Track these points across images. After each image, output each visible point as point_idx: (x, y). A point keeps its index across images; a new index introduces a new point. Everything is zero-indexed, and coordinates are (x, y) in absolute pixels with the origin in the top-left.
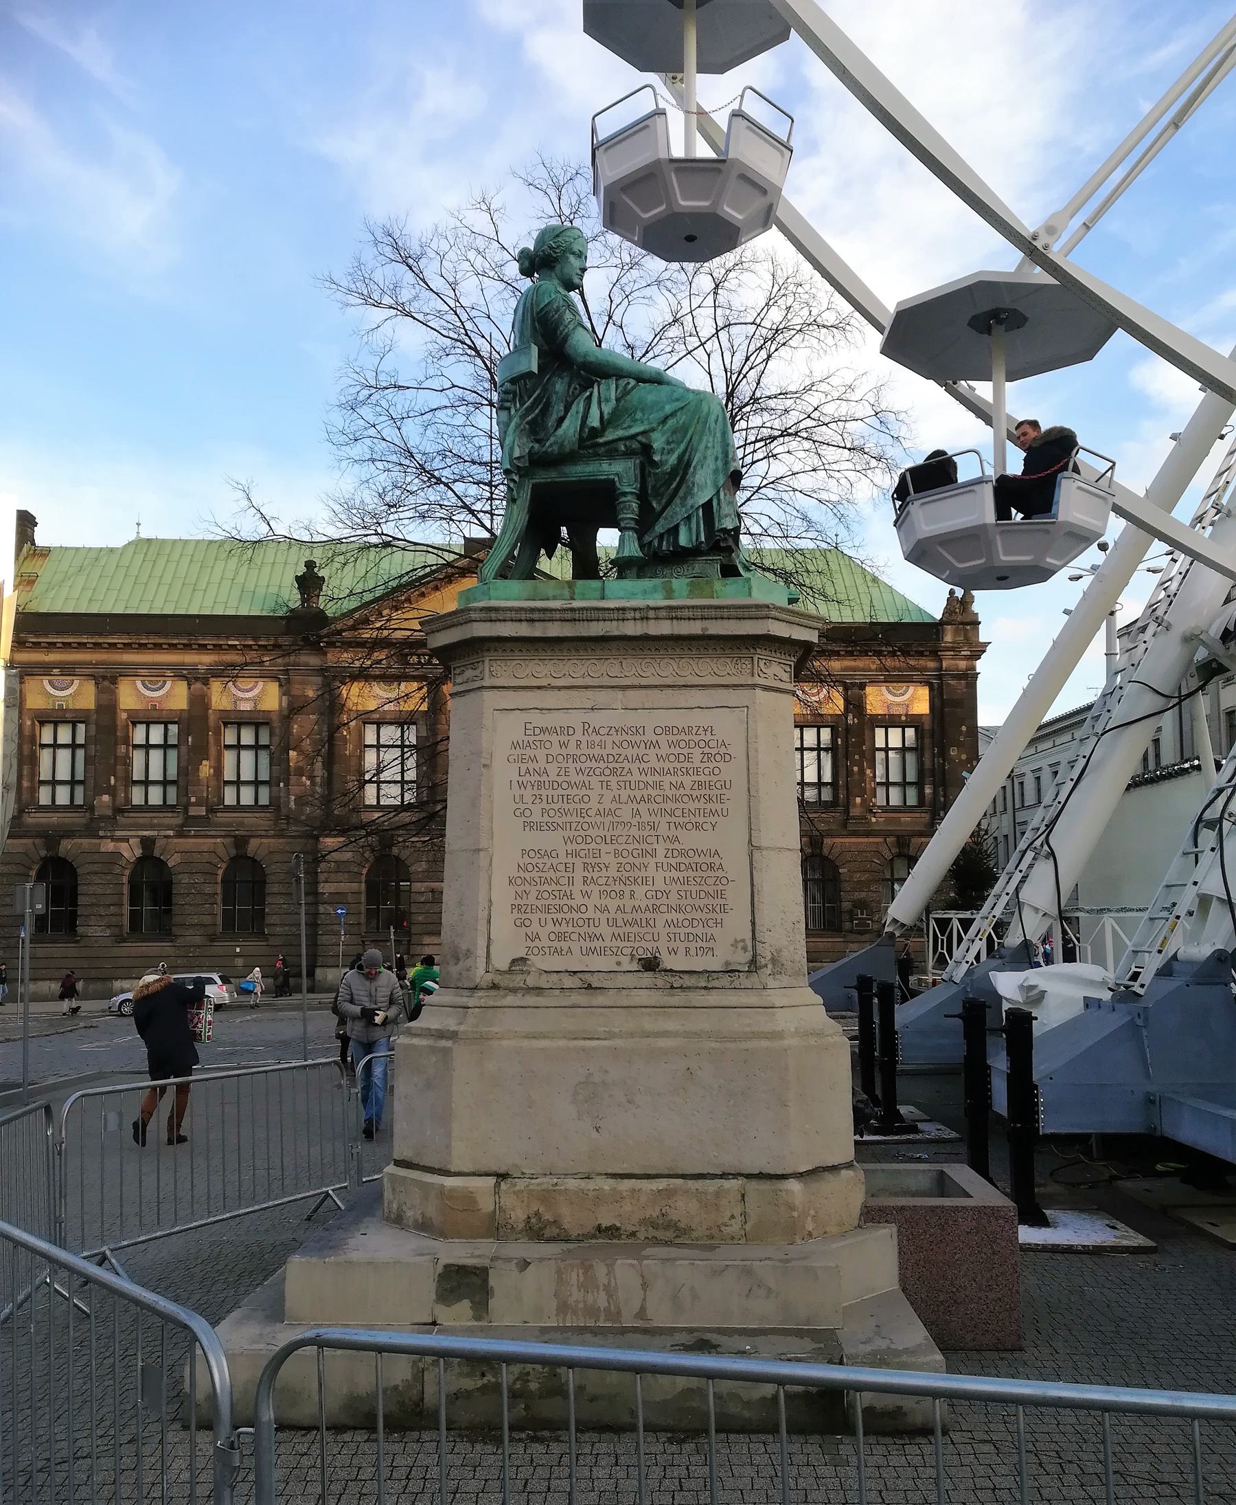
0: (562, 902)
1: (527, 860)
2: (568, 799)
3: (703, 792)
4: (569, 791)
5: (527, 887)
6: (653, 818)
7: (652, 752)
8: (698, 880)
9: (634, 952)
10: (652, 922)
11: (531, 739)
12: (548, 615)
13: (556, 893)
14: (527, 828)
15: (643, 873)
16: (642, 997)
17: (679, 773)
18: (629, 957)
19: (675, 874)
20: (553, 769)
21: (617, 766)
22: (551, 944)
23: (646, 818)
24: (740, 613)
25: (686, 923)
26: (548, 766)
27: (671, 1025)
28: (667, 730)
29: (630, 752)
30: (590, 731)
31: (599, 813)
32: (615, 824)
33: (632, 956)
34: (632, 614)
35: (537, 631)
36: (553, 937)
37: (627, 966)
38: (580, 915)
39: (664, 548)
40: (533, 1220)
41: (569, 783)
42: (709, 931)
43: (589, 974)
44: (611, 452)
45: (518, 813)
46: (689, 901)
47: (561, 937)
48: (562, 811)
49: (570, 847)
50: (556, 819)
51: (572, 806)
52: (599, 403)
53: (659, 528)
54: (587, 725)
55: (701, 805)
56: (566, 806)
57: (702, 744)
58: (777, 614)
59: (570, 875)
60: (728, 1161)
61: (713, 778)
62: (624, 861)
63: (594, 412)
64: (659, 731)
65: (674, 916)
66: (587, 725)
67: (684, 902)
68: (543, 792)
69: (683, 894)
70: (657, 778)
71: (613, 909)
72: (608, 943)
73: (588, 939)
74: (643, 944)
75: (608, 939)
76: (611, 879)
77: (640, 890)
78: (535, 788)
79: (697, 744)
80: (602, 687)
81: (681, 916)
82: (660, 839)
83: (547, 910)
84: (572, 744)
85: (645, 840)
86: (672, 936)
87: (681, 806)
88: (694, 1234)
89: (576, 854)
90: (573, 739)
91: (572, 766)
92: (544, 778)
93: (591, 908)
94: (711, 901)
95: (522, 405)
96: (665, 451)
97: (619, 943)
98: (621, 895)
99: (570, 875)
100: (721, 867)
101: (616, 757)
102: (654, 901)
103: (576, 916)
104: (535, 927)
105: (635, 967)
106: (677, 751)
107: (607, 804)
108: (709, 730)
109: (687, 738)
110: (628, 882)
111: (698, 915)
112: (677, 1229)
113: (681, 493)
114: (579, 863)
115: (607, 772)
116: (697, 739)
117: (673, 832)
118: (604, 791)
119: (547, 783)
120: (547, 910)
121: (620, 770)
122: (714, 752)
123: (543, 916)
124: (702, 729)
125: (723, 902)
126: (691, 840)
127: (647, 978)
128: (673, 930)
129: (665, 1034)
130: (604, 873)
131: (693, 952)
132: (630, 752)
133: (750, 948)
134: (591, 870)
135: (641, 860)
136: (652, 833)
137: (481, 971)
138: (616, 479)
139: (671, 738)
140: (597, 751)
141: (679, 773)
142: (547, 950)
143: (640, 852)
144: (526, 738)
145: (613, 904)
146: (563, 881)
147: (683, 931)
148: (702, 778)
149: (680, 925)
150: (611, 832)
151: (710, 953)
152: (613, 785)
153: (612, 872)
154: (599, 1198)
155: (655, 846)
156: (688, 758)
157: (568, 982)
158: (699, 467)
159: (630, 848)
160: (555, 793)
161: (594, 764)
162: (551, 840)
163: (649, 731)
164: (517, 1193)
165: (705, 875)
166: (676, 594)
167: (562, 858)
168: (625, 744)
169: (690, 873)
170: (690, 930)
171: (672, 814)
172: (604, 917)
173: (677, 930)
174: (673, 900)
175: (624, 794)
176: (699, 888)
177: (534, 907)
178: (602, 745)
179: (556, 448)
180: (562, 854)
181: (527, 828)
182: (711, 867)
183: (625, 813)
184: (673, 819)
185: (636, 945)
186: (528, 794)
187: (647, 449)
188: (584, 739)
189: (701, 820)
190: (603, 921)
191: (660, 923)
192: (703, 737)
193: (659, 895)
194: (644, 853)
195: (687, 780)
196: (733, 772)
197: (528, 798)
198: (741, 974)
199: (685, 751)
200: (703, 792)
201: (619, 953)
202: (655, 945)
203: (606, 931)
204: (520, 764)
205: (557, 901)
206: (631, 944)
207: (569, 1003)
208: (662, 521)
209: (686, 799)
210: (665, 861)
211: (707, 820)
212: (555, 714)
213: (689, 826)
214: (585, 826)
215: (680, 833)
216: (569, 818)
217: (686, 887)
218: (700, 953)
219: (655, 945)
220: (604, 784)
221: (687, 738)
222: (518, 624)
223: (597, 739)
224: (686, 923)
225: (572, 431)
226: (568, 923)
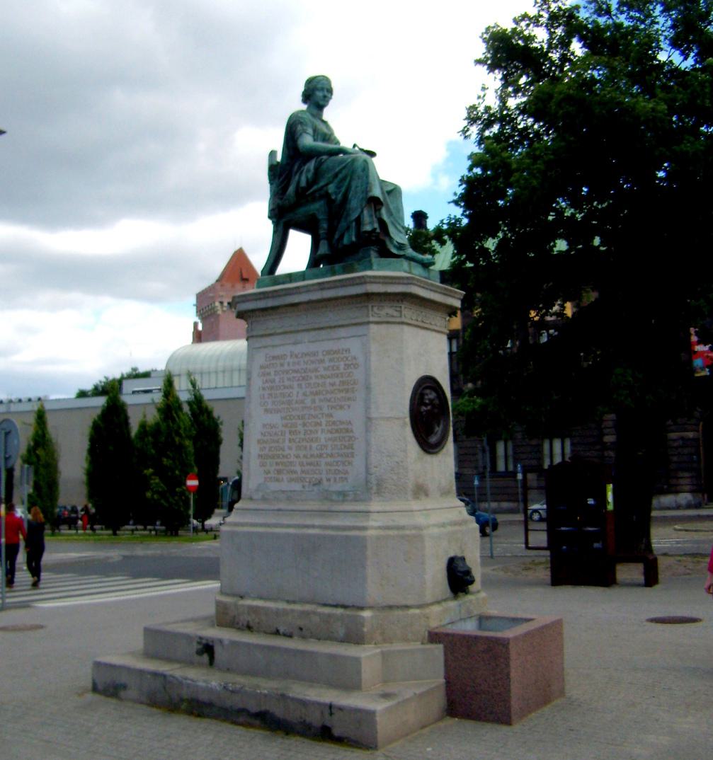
5: (265, 445)
20: (277, 379)
23: (318, 403)
28: (328, 352)
29: (312, 366)
31: (297, 402)
42: (346, 468)
44: (313, 198)
45: (262, 404)
47: (279, 472)
55: (343, 394)
61: (349, 379)
65: (329, 460)
67: (334, 451)
71: (301, 456)
74: (316, 476)
77: (314, 445)
83: (273, 457)
94: (346, 451)
97: (304, 475)
100: (352, 431)
103: (285, 460)
106: (332, 364)
108: (348, 350)
111: (340, 459)
116: (342, 356)
120: (273, 457)
122: (350, 363)
126: (340, 415)
128: (329, 467)
129: (313, 527)
132: (312, 366)
136: (321, 412)
138: (316, 212)
140: (297, 367)
145: (302, 453)
146: (281, 441)
147: (333, 468)
148: (344, 379)
156: (338, 368)
159: (310, 421)
161: (295, 375)
162: (275, 419)
165: (344, 435)
169: (337, 435)
170: (337, 467)
171: (329, 401)
174: (329, 451)
175: (308, 390)
176: (341, 443)
178: (298, 363)
182: (347, 431)
183: (308, 401)
184: (330, 404)
186: (267, 392)
189: (343, 403)
192: (345, 355)
195: (337, 381)
196: (358, 375)
197: (266, 396)
203: (298, 468)
207: (276, 507)
217: (335, 443)
223: (296, 360)
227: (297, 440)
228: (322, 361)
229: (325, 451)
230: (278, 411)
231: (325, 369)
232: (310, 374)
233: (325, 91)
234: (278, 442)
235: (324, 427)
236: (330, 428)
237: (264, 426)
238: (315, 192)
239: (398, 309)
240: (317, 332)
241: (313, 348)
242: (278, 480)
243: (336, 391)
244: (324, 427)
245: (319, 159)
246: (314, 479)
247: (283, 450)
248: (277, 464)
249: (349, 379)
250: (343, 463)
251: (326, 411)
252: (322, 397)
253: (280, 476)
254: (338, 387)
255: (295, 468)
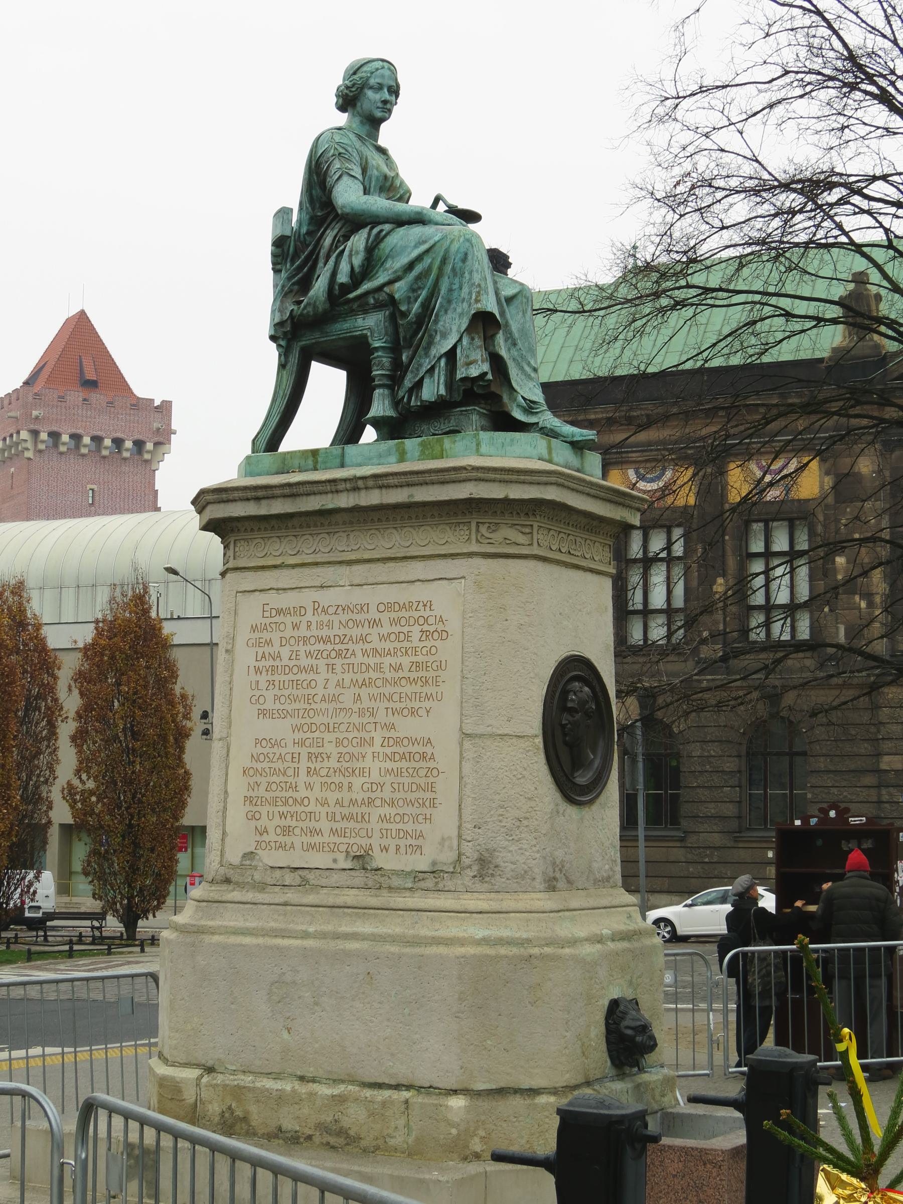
0: (288, 794)
1: (259, 750)
2: (297, 684)
3: (420, 674)
4: (299, 676)
5: (258, 779)
6: (373, 704)
7: (375, 631)
8: (411, 771)
9: (349, 849)
10: (366, 817)
11: (268, 621)
12: (270, 492)
13: (283, 785)
14: (261, 716)
15: (360, 765)
16: (350, 897)
17: (399, 653)
18: (344, 854)
19: (389, 765)
20: (285, 652)
21: (343, 647)
22: (276, 838)
23: (366, 703)
24: (441, 477)
25: (398, 819)
26: (282, 650)
27: (366, 928)
28: (389, 607)
29: (356, 632)
30: (320, 610)
31: (323, 699)
32: (338, 711)
33: (347, 852)
34: (344, 486)
35: (263, 509)
36: (278, 830)
37: (343, 864)
38: (302, 808)
39: (412, 403)
40: (227, 1115)
41: (299, 667)
42: (419, 827)
43: (307, 871)
44: (363, 306)
45: (253, 701)
46: (402, 795)
47: (287, 831)
48: (291, 697)
49: (298, 736)
50: (286, 706)
51: (300, 692)
52: (350, 256)
53: (408, 383)
54: (316, 604)
55: (417, 688)
56: (295, 692)
57: (421, 621)
58: (479, 475)
59: (295, 765)
60: (402, 1071)
61: (431, 659)
62: (344, 750)
63: (344, 267)
64: (382, 608)
65: (387, 810)
66: (316, 604)
67: (397, 795)
68: (276, 677)
69: (396, 786)
70: (378, 660)
71: (332, 802)
72: (326, 839)
73: (309, 834)
74: (358, 841)
75: (326, 834)
76: (332, 770)
77: (357, 782)
78: (270, 673)
79: (417, 621)
80: (329, 563)
81: (393, 811)
82: (378, 726)
84: (304, 626)
85: (363, 726)
86: (384, 832)
87: (400, 690)
88: (363, 1143)
89: (302, 743)
90: (304, 619)
91: (302, 648)
92: (277, 663)
93: (313, 801)
94: (420, 794)
95: (292, 265)
96: (412, 300)
97: (338, 840)
98: (340, 787)
99: (295, 765)
100: (432, 757)
101: (342, 638)
102: (369, 794)
103: (300, 809)
104: (264, 822)
105: (349, 865)
106: (397, 629)
107: (332, 690)
108: (427, 605)
109: (407, 615)
110: (347, 774)
112: (348, 1136)
113: (424, 343)
114: (304, 751)
115: (333, 654)
116: (416, 615)
117: (391, 719)
118: (330, 675)
119: (280, 668)
120: (274, 802)
121: (345, 652)
122: (432, 629)
123: (271, 809)
124: (421, 604)
125: (433, 795)
126: (408, 727)
127: (359, 878)
128: (386, 826)
129: (354, 936)
130: (326, 764)
131: (403, 850)
132: (356, 632)
133: (456, 847)
134: (314, 760)
135: (359, 749)
136: (372, 720)
137: (215, 865)
138: (369, 334)
139: (393, 615)
140: (325, 632)
141: (399, 653)
142: (273, 844)
143: (359, 740)
144: (264, 621)
145: (332, 797)
146: (290, 772)
147: (394, 827)
148: (420, 658)
149: (392, 820)
150: (334, 720)
151: (418, 852)
152: (338, 669)
153: (333, 763)
154: (281, 1098)
155: (373, 734)
156: (408, 637)
157: (289, 878)
158: (442, 313)
160: (286, 678)
161: (321, 646)
162: (280, 729)
163: (373, 608)
164: (215, 1086)
165: (417, 765)
166: (409, 455)
167: (291, 749)
168: (351, 624)
169: (404, 764)
170: (400, 826)
172: (324, 810)
173: (389, 826)
174: (387, 794)
175: (348, 677)
176: (410, 780)
177: (264, 799)
178: (329, 625)
179: (310, 309)
180: (290, 744)
181: (261, 716)
182: (423, 756)
184: (391, 705)
185: (352, 841)
187: (392, 301)
188: (314, 620)
189: (416, 705)
190: (323, 815)
191: (374, 818)
192: (422, 613)
193: (374, 787)
194: (363, 742)
195: (406, 661)
197: (263, 685)
198: (446, 875)
199: (405, 629)
200: (420, 674)
201: (336, 849)
202: (369, 841)
203: (325, 825)
204: (258, 649)
205: (284, 794)
206: (346, 840)
208: (409, 376)
209: (403, 682)
210: (381, 750)
211: (423, 705)
212: (290, 594)
213: (405, 712)
214: (312, 713)
215: (396, 719)
216: (297, 706)
217: (400, 780)
218: (409, 851)
219: (369, 841)
220: (330, 667)
221: (407, 615)
222: (247, 503)
223: (325, 618)
224: (398, 819)
225: (321, 290)
226: (292, 816)
227: (324, 772)
228: (376, 623)
229: (378, 794)
230: (285, 714)
231: (382, 638)
232: (351, 646)
233: (386, 90)
234: (284, 774)
235: (377, 747)
236: (388, 751)
237: (258, 742)
238: (367, 293)
239: (527, 530)
240: (367, 566)
241: (359, 596)
242: (282, 847)
243: (403, 682)
244: (377, 747)
245: (375, 231)
246: (355, 848)
247: (295, 789)
248: (282, 815)
249: (431, 659)
250: (415, 818)
251: (381, 717)
252: (374, 691)
253: (288, 840)
254: (407, 675)
255: (317, 826)
